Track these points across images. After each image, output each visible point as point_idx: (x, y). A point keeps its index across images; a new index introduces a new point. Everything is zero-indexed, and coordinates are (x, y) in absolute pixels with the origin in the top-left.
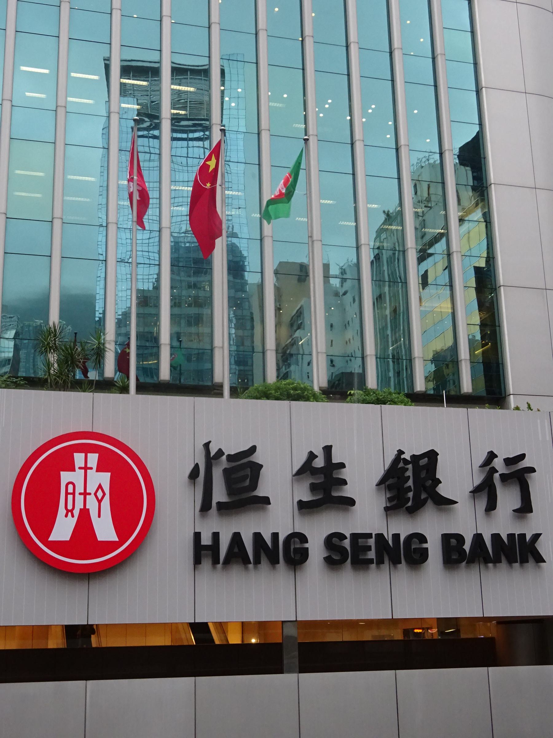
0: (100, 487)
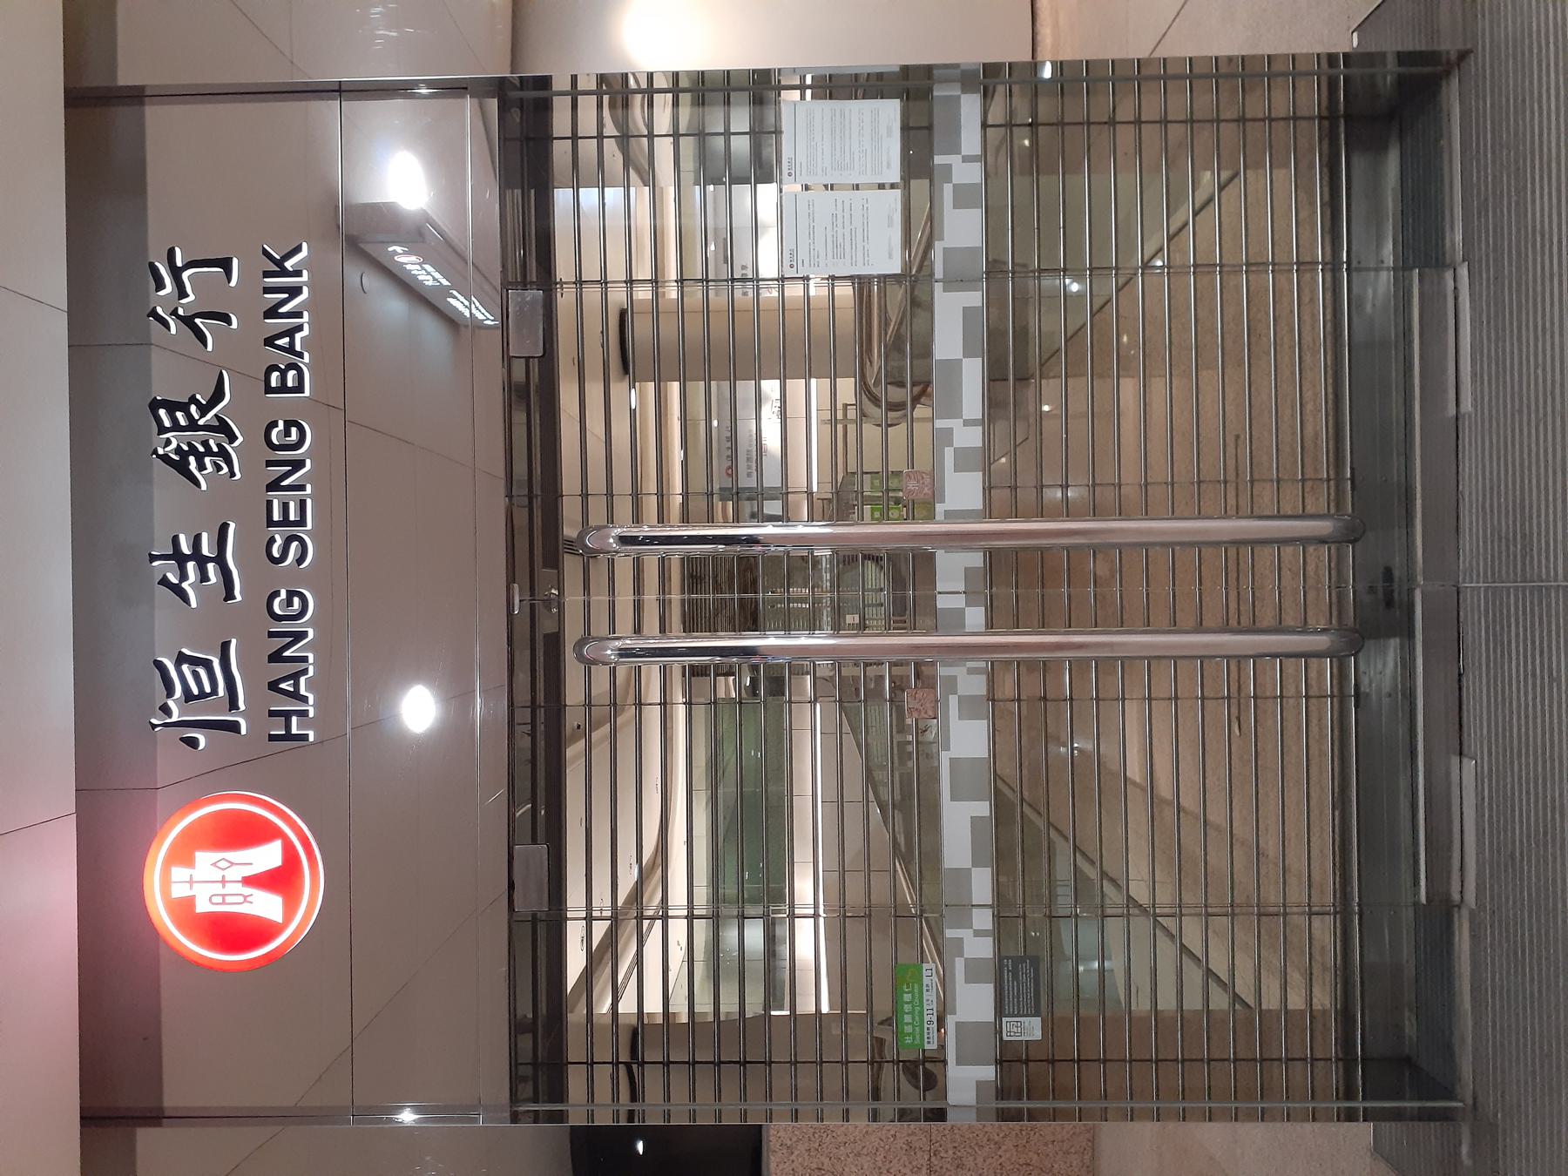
0: (214, 864)
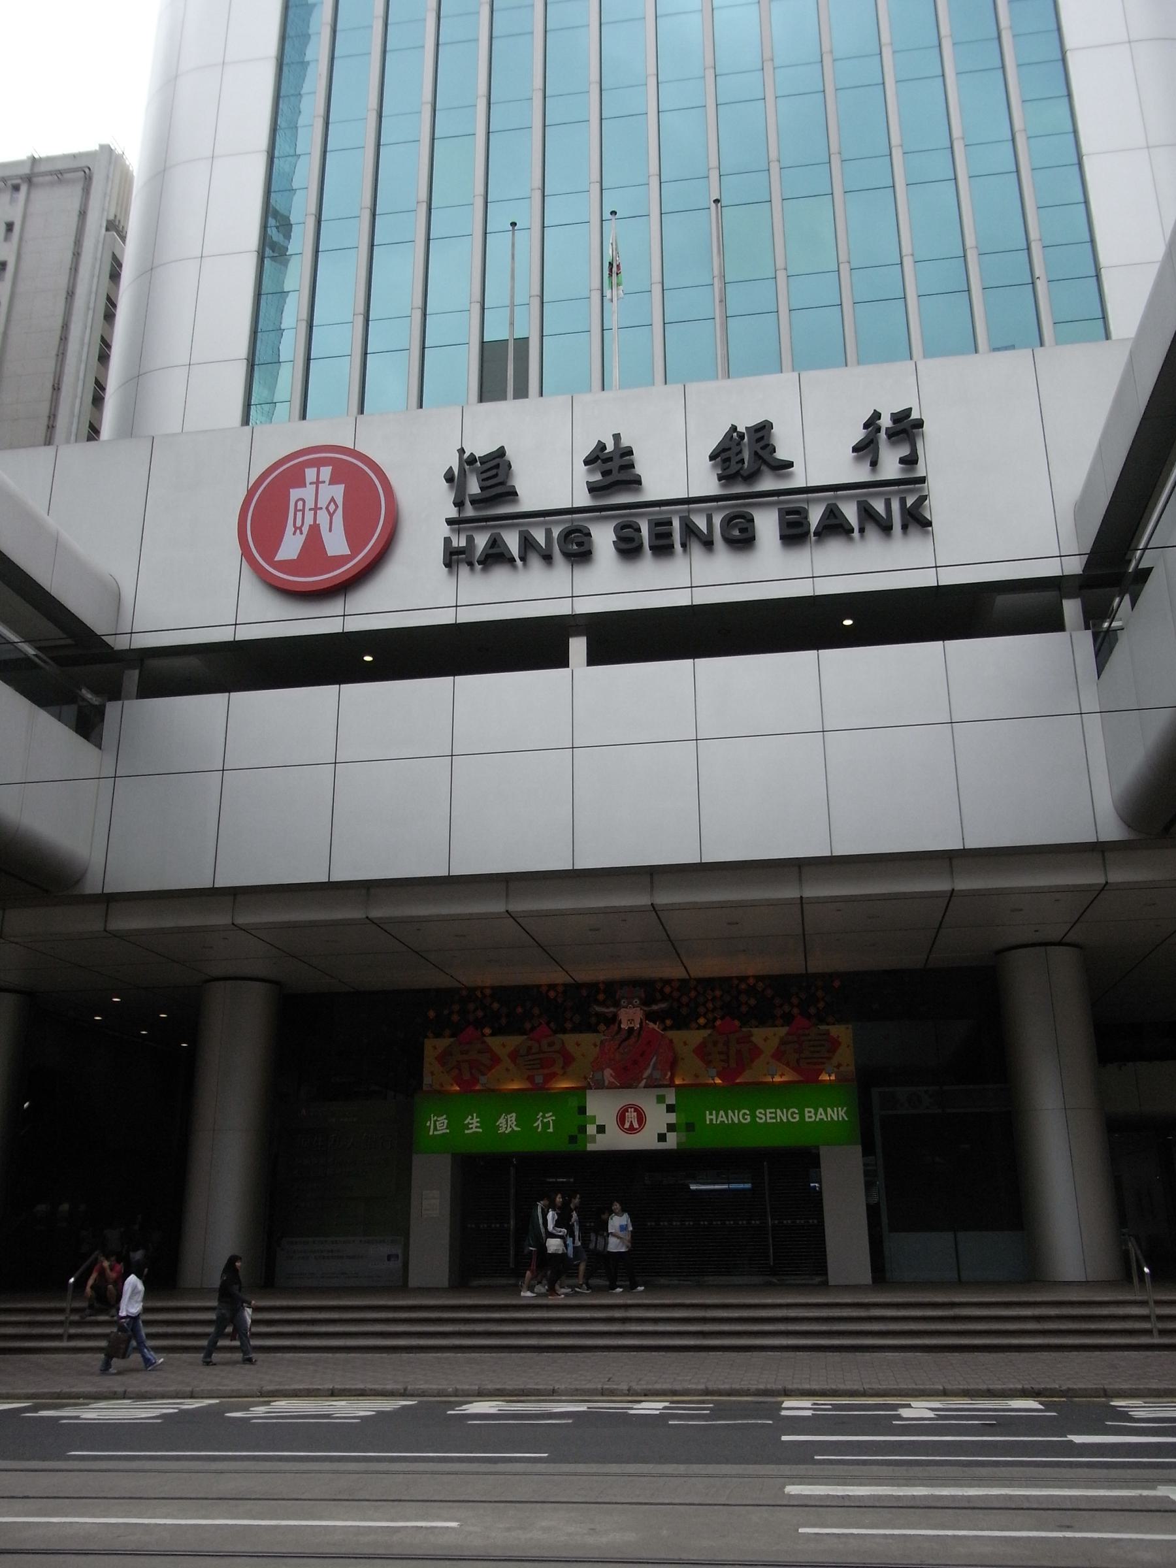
0: (333, 500)
